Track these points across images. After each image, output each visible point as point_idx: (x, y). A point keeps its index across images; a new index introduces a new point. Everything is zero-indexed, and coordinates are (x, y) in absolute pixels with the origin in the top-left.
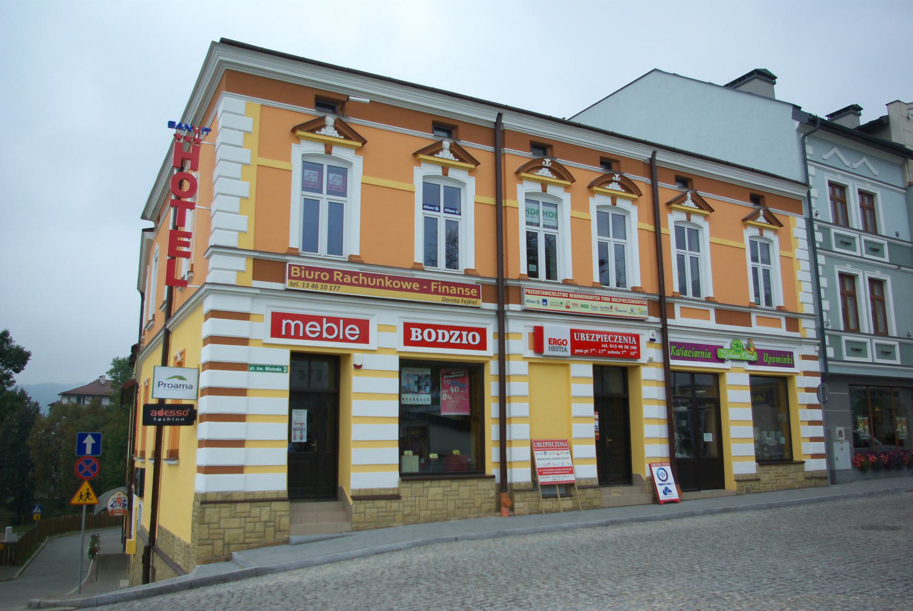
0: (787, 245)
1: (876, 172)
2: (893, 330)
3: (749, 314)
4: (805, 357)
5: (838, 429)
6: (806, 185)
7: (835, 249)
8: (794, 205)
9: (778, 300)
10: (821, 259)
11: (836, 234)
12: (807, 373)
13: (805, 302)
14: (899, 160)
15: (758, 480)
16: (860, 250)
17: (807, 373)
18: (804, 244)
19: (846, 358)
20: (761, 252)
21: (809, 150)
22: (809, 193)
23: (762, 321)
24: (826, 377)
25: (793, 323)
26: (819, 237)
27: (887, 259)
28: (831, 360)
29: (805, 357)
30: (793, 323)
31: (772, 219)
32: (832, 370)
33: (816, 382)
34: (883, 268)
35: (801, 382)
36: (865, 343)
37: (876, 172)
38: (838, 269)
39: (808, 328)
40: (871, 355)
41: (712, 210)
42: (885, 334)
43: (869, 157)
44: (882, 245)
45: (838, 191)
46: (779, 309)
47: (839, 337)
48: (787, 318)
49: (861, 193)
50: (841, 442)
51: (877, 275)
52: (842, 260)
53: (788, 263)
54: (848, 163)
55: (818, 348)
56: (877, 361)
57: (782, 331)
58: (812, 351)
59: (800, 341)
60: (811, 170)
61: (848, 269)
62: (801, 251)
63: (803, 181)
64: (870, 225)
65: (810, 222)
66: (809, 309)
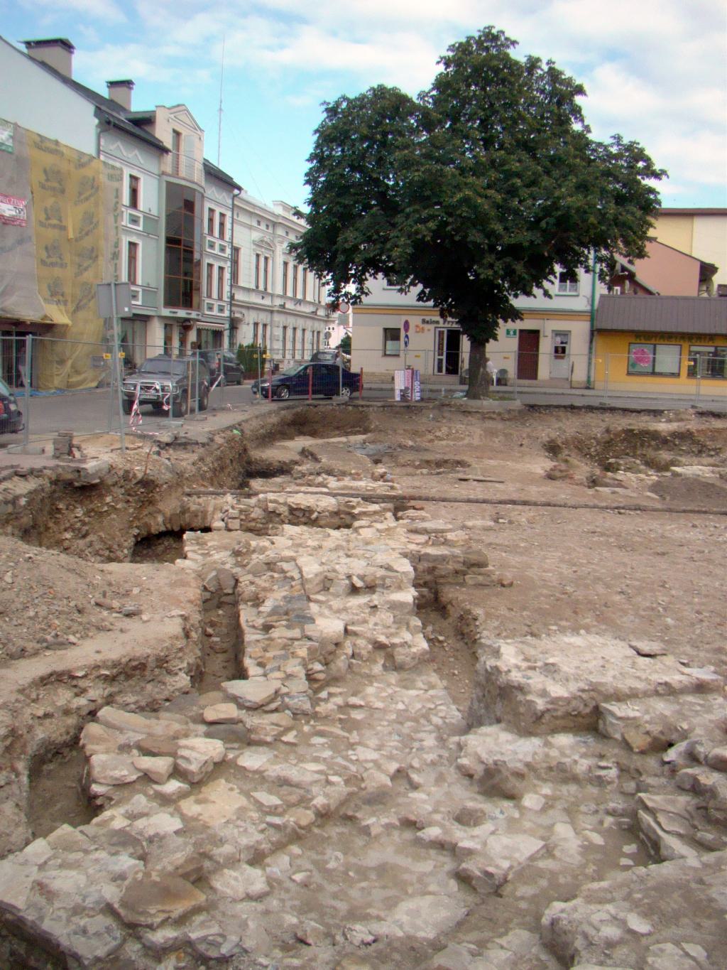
2: (139, 281)
21: (103, 142)
27: (141, 228)
34: (138, 234)
42: (134, 283)
51: (134, 239)
54: (125, 154)
64: (134, 203)
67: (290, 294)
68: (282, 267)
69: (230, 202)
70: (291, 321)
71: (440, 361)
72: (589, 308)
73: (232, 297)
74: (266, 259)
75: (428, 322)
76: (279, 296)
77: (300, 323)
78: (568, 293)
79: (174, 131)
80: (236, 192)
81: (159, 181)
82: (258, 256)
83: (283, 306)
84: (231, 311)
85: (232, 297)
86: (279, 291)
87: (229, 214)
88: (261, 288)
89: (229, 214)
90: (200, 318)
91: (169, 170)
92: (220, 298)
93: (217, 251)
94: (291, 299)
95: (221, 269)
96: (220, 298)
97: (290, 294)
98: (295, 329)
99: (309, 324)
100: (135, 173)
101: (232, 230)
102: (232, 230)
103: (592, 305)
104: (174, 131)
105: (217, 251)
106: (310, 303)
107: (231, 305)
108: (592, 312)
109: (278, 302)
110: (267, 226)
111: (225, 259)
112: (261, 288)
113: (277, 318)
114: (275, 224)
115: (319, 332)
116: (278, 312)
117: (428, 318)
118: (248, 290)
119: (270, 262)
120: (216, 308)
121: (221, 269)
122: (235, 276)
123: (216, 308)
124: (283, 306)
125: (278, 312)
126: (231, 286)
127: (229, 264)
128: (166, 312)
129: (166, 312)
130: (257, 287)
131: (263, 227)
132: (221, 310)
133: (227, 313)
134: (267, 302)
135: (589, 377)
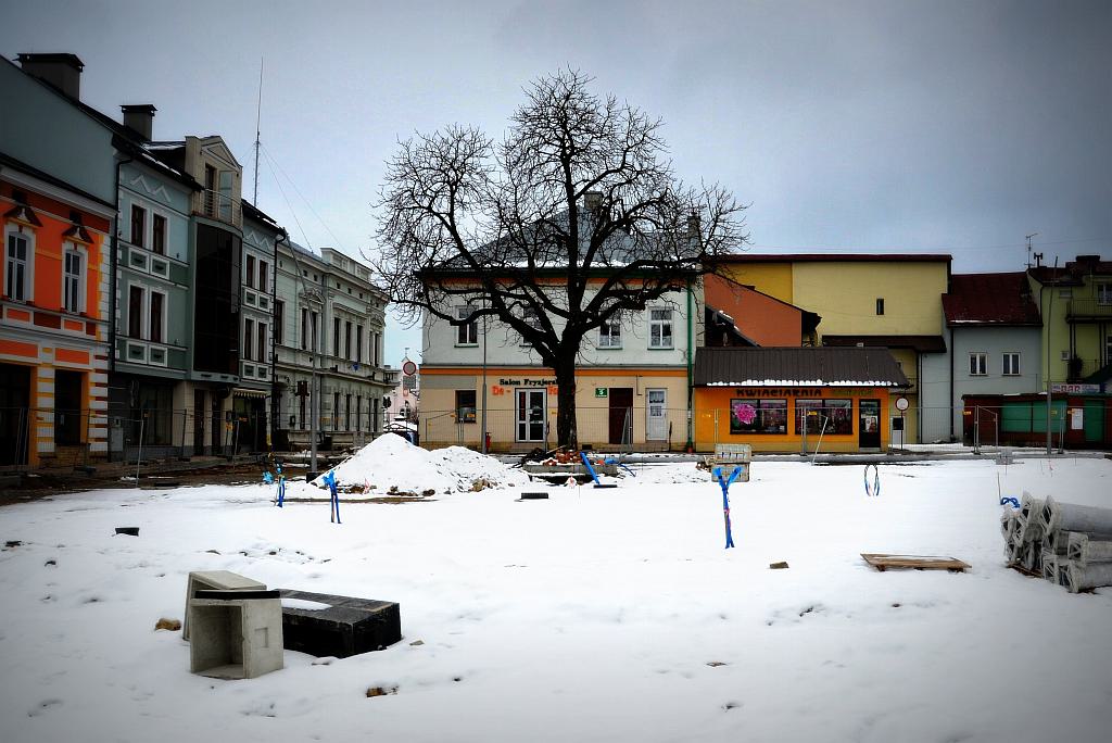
0: (94, 259)
1: (169, 200)
2: (165, 337)
3: (59, 318)
4: (97, 357)
5: (118, 418)
6: (115, 207)
7: (130, 266)
8: (103, 224)
9: (83, 306)
10: (119, 274)
11: (133, 253)
12: (98, 371)
13: (103, 307)
14: (188, 191)
15: (55, 457)
16: (148, 269)
17: (98, 371)
18: (107, 259)
19: (129, 360)
20: (73, 263)
21: (121, 176)
22: (117, 216)
23: (69, 325)
24: (112, 373)
25: (91, 329)
26: (119, 254)
28: (118, 360)
29: (97, 357)
30: (91, 329)
31: (86, 237)
32: (117, 369)
33: (104, 378)
35: (94, 378)
36: (143, 348)
37: (169, 200)
38: (131, 283)
39: (103, 332)
40: (147, 359)
41: (40, 225)
43: (167, 186)
44: (165, 264)
45: (138, 214)
46: (82, 315)
47: (125, 341)
48: (87, 323)
49: (155, 216)
50: (117, 429)
51: (158, 290)
52: (135, 276)
53: (93, 276)
55: (108, 350)
56: (151, 363)
57: (83, 334)
58: (103, 352)
59: (96, 343)
60: (121, 194)
61: (138, 284)
62: (104, 267)
63: (113, 204)
64: (159, 248)
65: (114, 240)
66: (105, 316)
67: (342, 355)
69: (273, 249)
70: (344, 386)
71: (522, 427)
72: (685, 362)
73: (275, 359)
74: (314, 314)
75: (507, 383)
76: (332, 358)
77: (355, 387)
78: (661, 346)
79: (207, 166)
80: (280, 237)
81: (190, 223)
82: (304, 311)
83: (335, 370)
84: (273, 375)
85: (275, 359)
86: (330, 351)
87: (271, 262)
88: (309, 348)
89: (271, 262)
90: (238, 382)
91: (201, 209)
92: (261, 360)
93: (257, 305)
94: (344, 361)
95: (262, 326)
96: (261, 360)
97: (342, 355)
98: (348, 396)
99: (365, 389)
100: (162, 214)
101: (275, 281)
102: (275, 281)
103: (689, 359)
104: (207, 166)
105: (257, 305)
106: (366, 366)
107: (274, 368)
108: (689, 366)
109: (330, 365)
111: (266, 315)
114: (324, 276)
115: (376, 401)
116: (329, 376)
117: (506, 379)
118: (294, 351)
120: (256, 371)
121: (262, 326)
122: (278, 335)
123: (256, 371)
124: (335, 370)
125: (329, 376)
126: (274, 346)
127: (271, 320)
128: (197, 376)
129: (197, 376)
130: (304, 347)
131: (310, 278)
132: (262, 373)
133: (269, 378)
135: (689, 438)
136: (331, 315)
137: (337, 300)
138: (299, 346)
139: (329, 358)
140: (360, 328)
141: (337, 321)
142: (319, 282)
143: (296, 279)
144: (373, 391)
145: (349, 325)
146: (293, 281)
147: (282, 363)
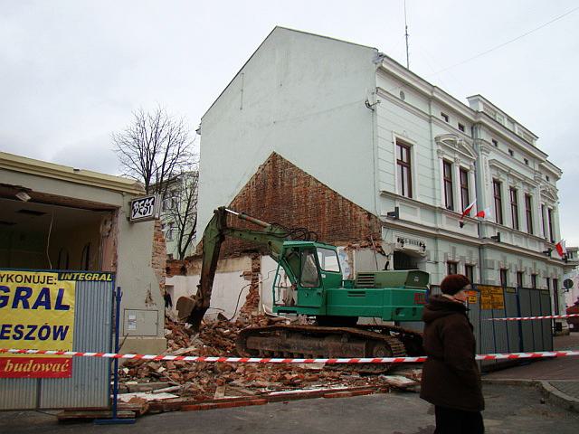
67: (508, 223)
68: (491, 185)
70: (512, 261)
74: (464, 172)
77: (527, 264)
82: (447, 164)
83: (497, 238)
86: (490, 214)
94: (511, 231)
97: (508, 223)
99: (541, 267)
106: (540, 240)
109: (490, 233)
110: (461, 127)
112: (458, 208)
113: (491, 256)
114: (475, 126)
115: (555, 281)
118: (433, 210)
119: (472, 177)
124: (497, 238)
130: (451, 207)
134: (471, 231)
136: (487, 176)
137: (492, 156)
138: (441, 203)
139: (488, 224)
140: (528, 198)
141: (497, 183)
142: (468, 131)
143: (430, 119)
144: (551, 270)
145: (514, 191)
146: (425, 124)
147: (402, 221)
